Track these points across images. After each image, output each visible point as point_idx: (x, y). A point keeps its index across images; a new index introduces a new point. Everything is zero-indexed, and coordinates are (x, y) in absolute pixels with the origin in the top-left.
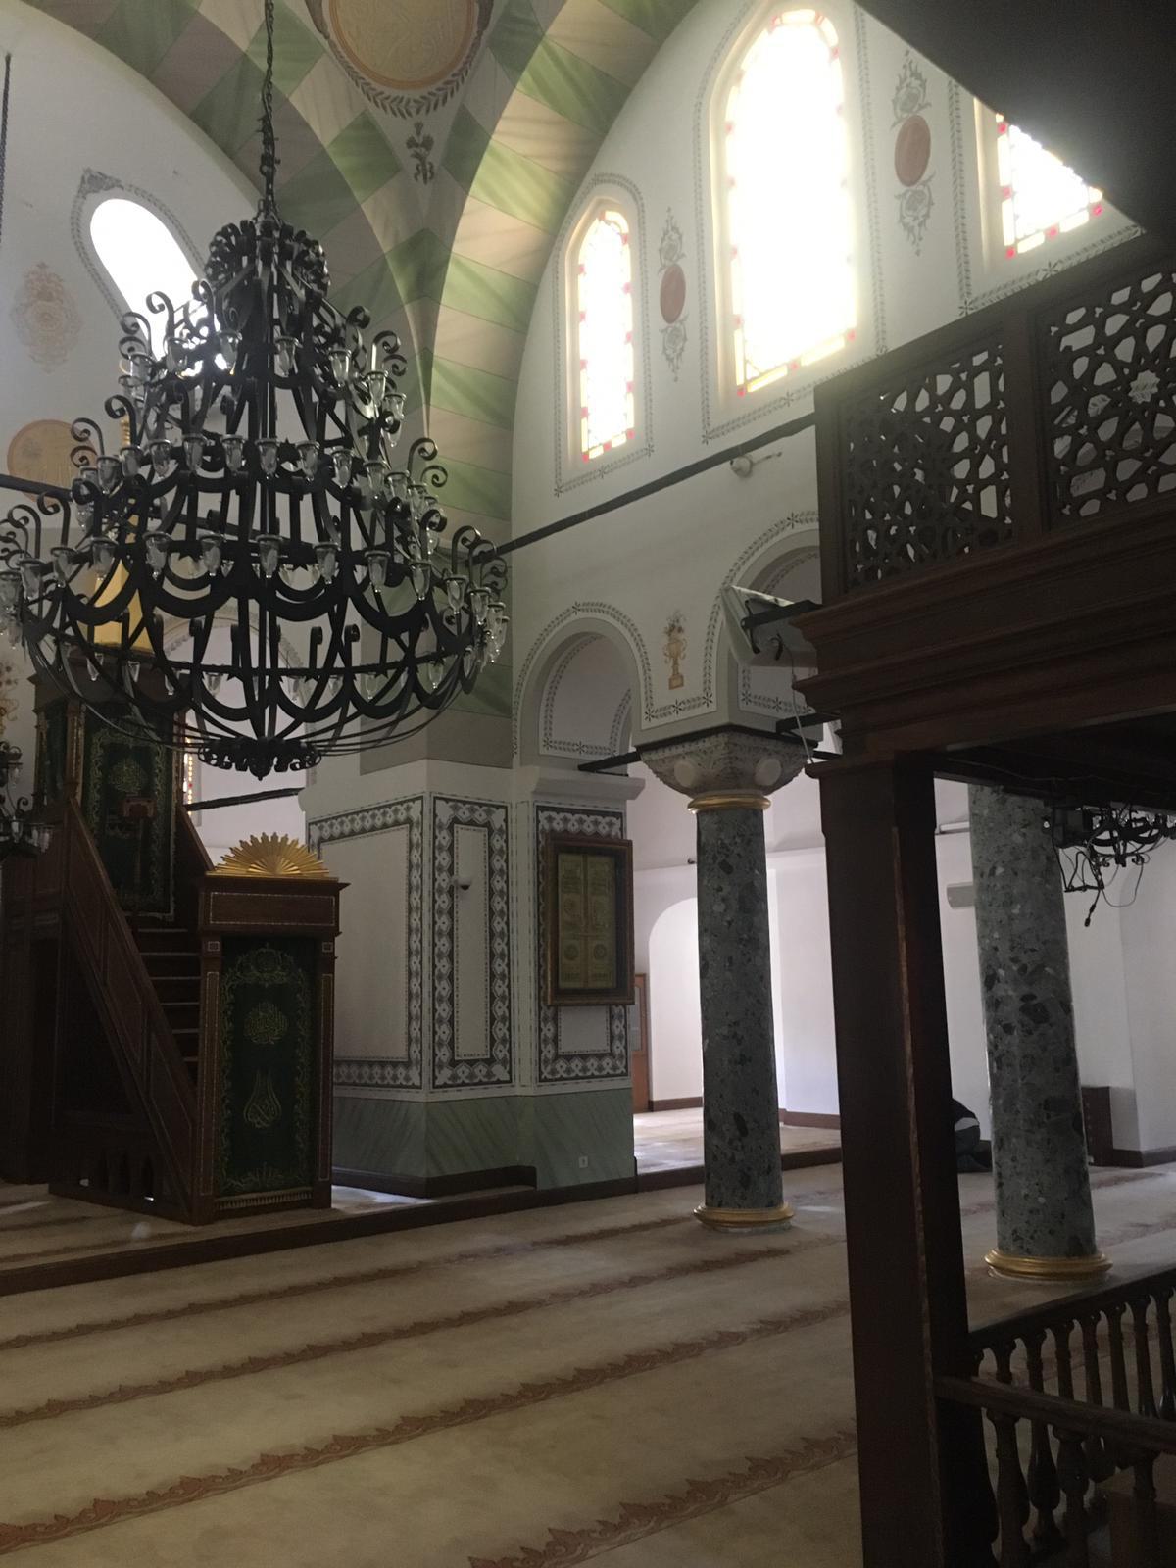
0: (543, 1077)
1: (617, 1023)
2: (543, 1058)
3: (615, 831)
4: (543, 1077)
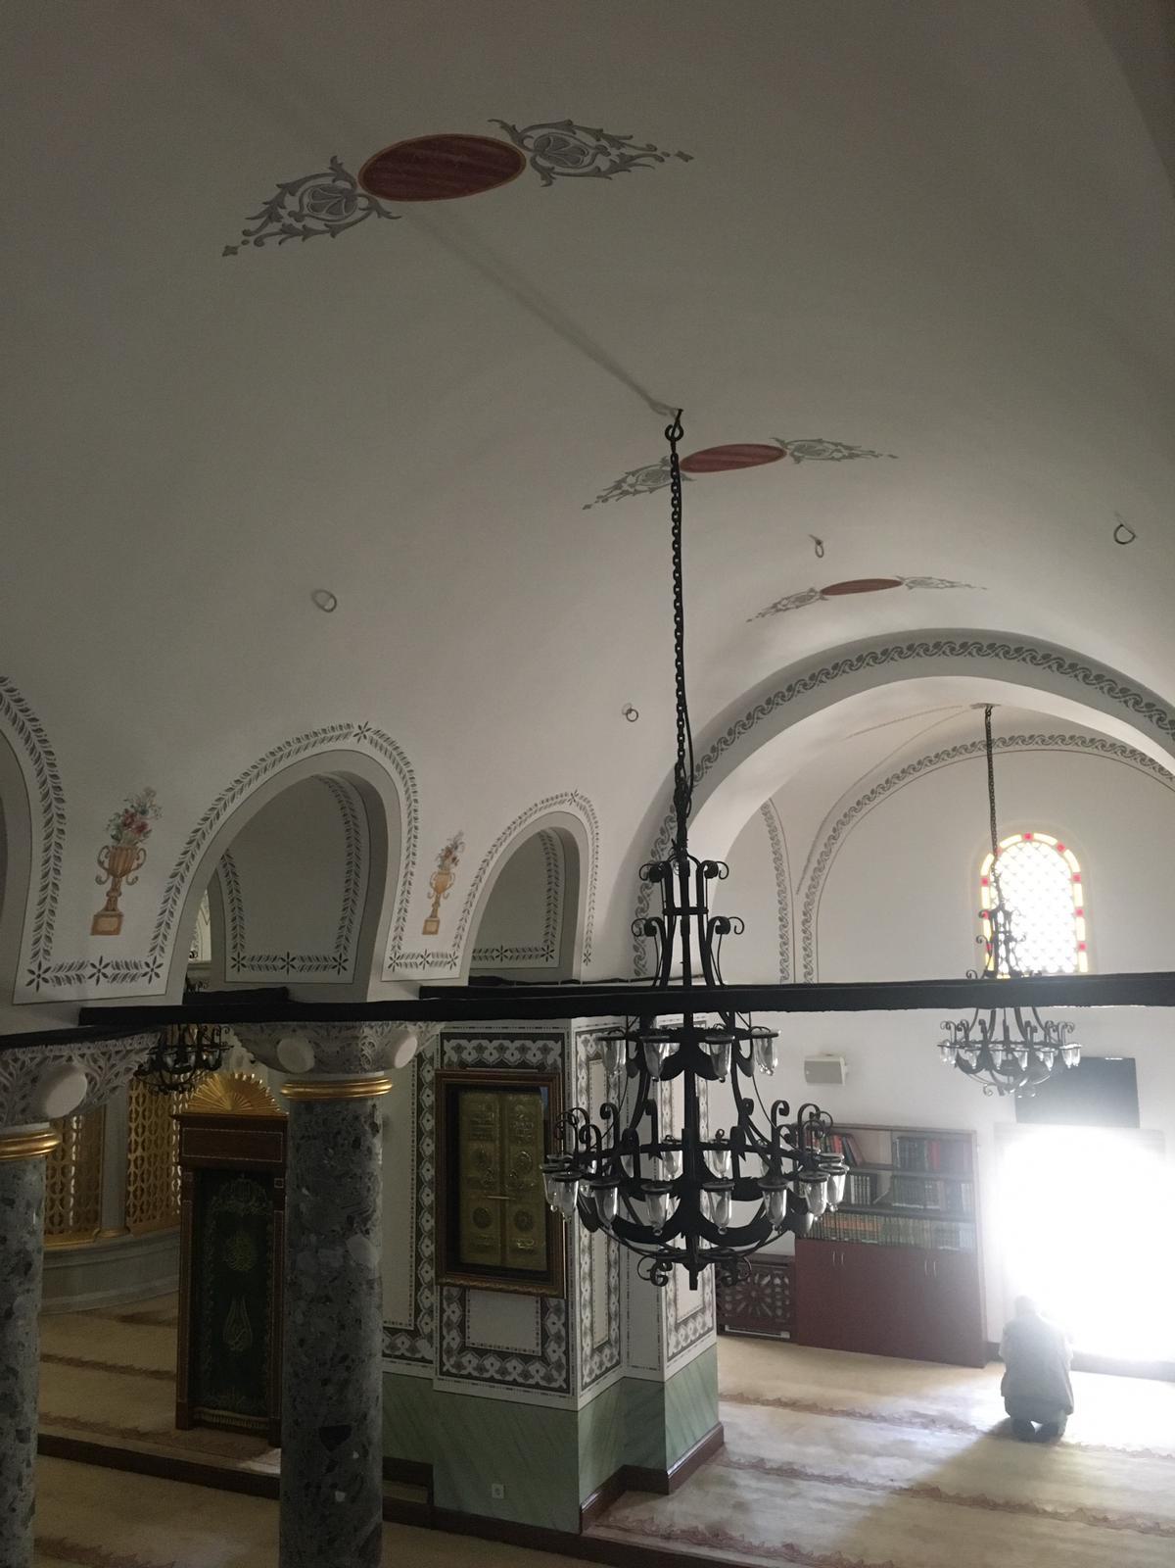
0: (445, 1369)
1: (553, 1318)
2: (445, 1346)
3: (553, 1058)
4: (445, 1369)
